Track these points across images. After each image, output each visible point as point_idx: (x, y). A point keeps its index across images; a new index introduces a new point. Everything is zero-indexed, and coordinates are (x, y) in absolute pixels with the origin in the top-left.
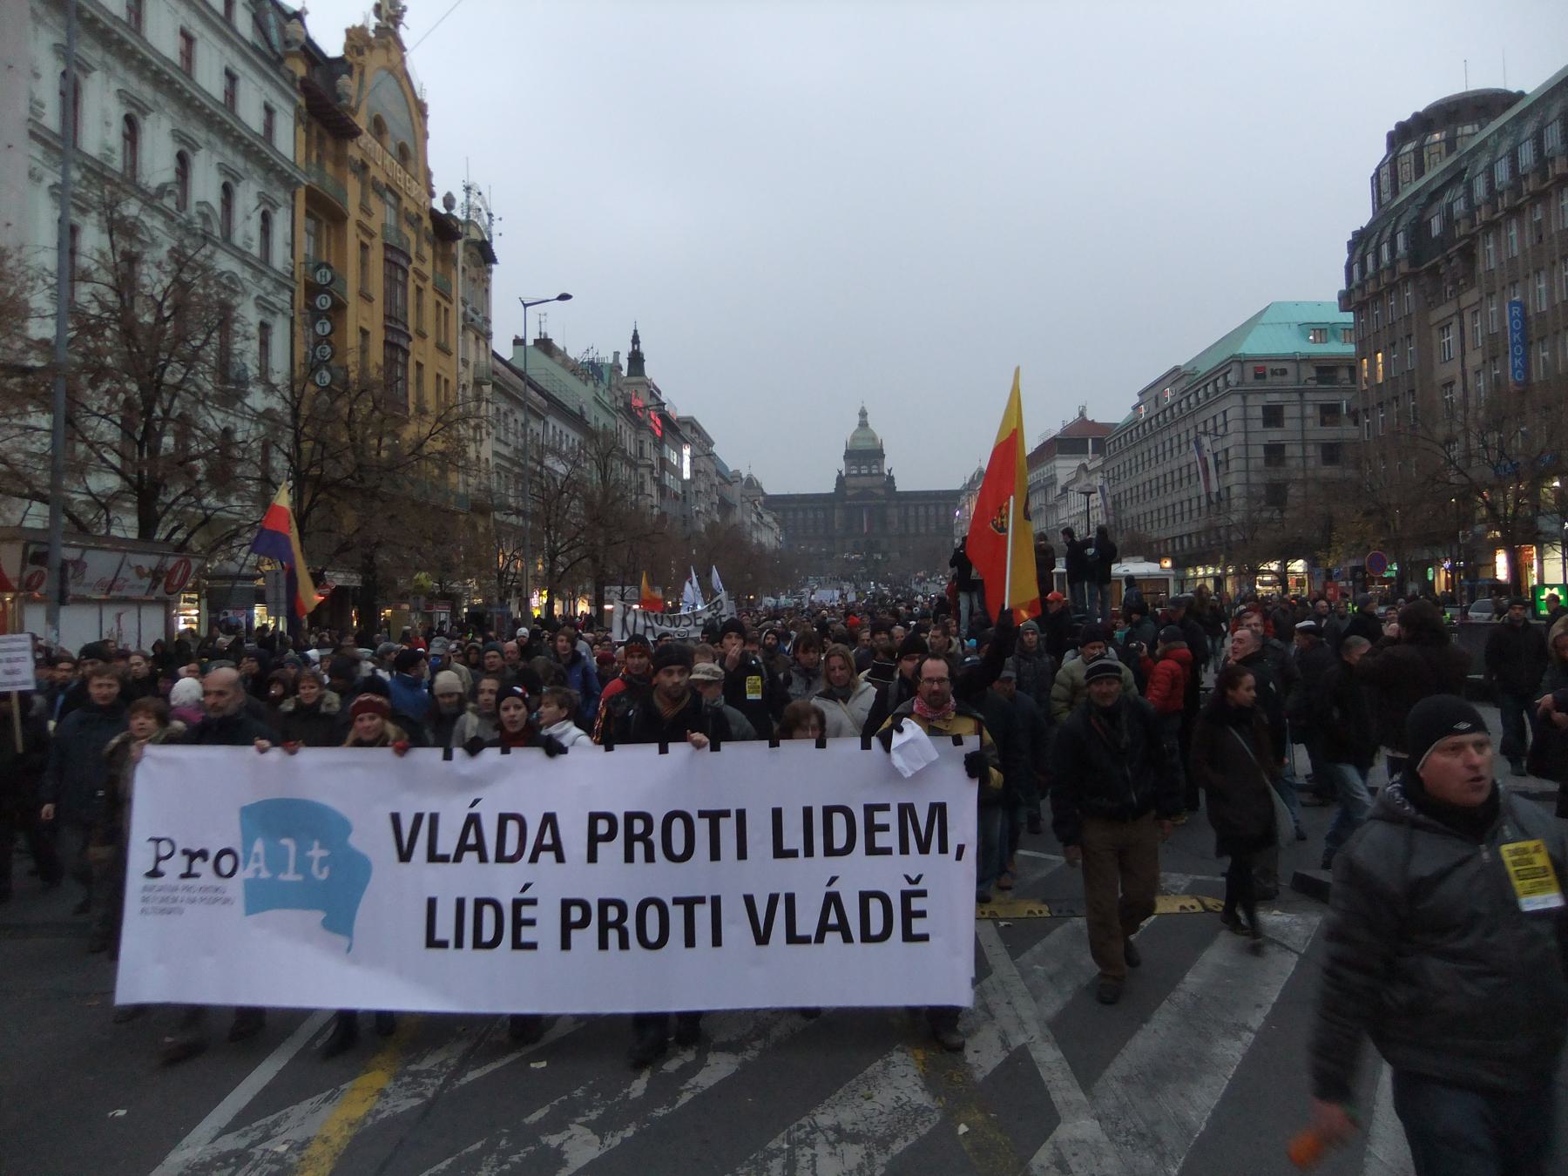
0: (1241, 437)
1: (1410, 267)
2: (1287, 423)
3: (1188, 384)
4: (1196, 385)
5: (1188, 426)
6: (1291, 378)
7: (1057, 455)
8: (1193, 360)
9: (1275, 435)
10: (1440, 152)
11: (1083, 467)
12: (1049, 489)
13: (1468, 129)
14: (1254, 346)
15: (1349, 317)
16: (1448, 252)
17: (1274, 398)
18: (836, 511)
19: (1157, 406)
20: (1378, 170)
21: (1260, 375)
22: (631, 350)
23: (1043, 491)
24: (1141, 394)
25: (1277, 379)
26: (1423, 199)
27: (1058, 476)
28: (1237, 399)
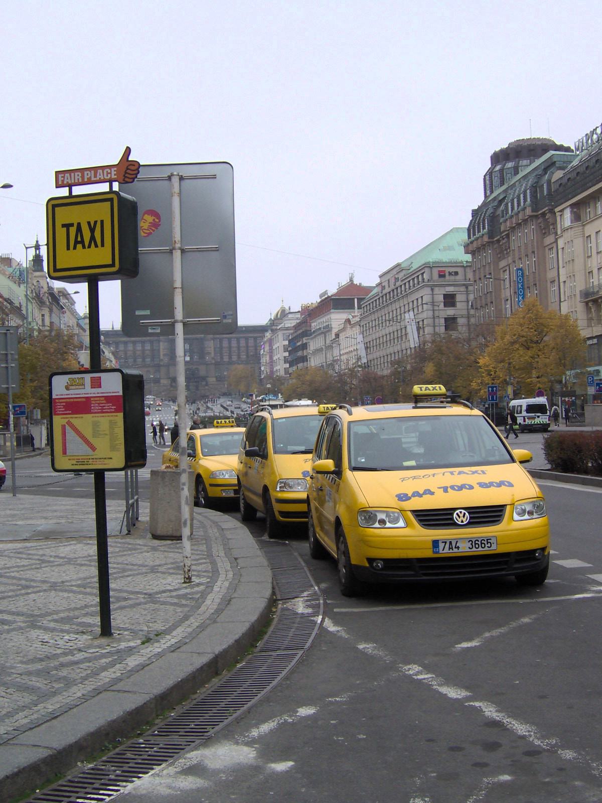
0: (430, 313)
1: (489, 238)
2: (458, 304)
3: (405, 275)
4: (408, 277)
5: (405, 303)
6: (460, 277)
7: (332, 311)
8: (411, 257)
9: (450, 312)
10: (511, 173)
11: (348, 321)
12: (327, 334)
13: (525, 162)
14: (435, 256)
15: (469, 257)
16: (503, 235)
17: (450, 289)
18: (161, 344)
19: (389, 286)
20: (485, 176)
21: (442, 275)
22: (34, 254)
23: (323, 335)
24: (380, 277)
25: (452, 278)
26: (496, 203)
27: (333, 326)
28: (427, 291)
